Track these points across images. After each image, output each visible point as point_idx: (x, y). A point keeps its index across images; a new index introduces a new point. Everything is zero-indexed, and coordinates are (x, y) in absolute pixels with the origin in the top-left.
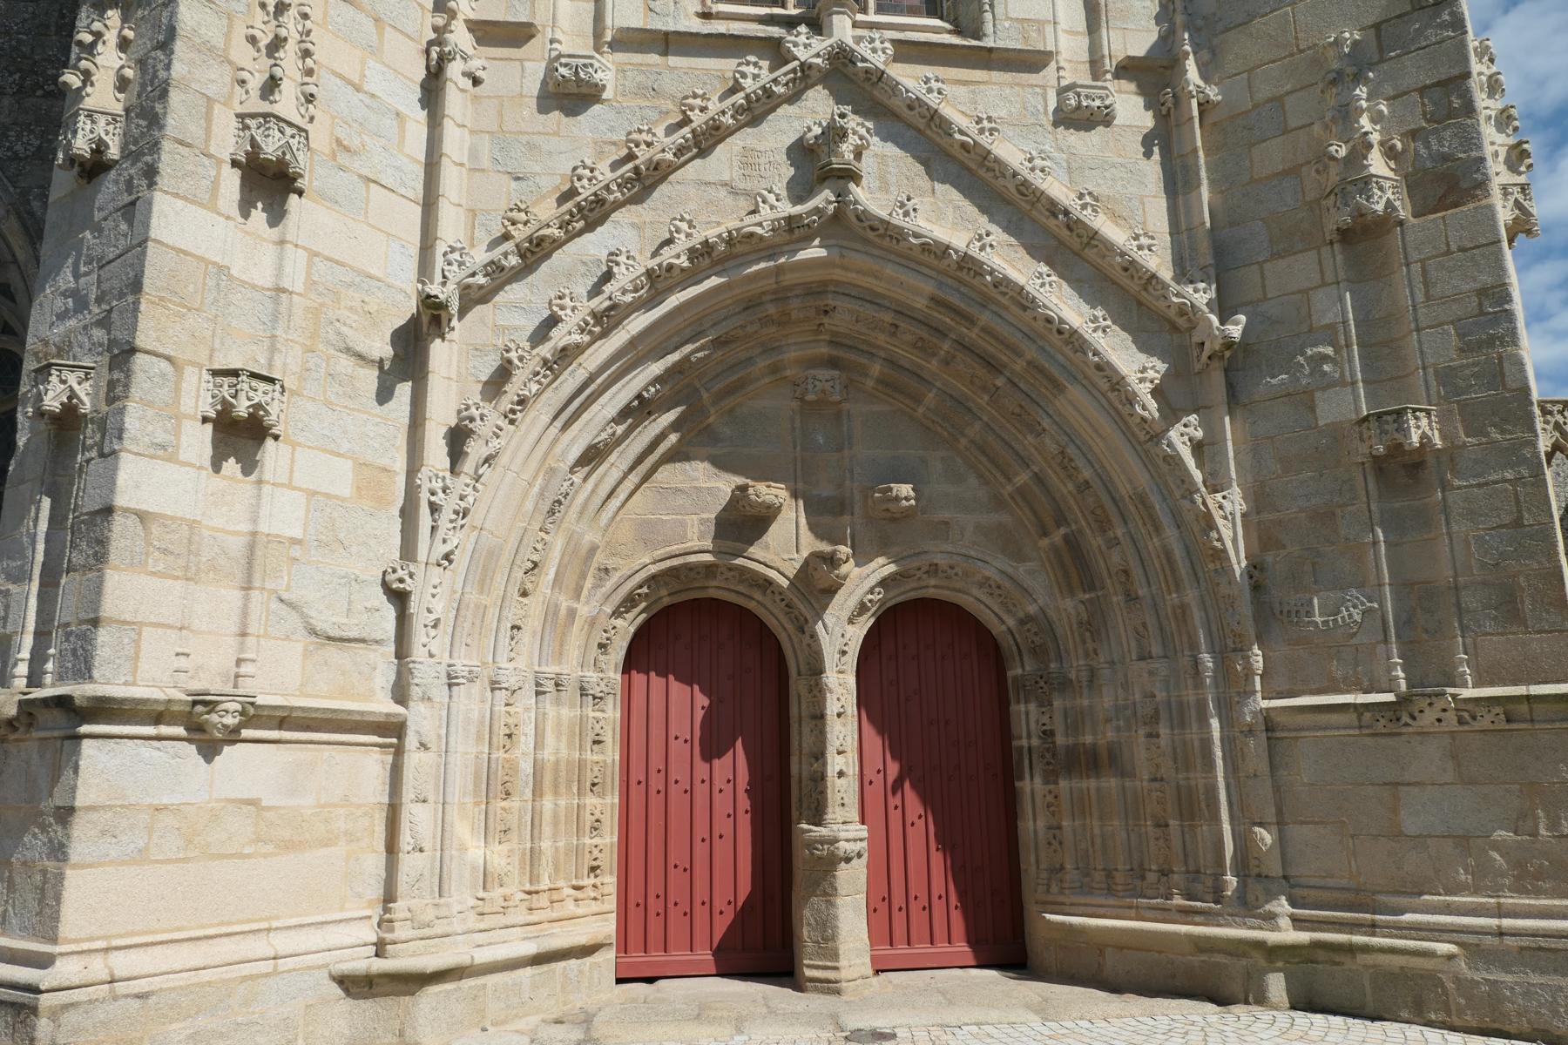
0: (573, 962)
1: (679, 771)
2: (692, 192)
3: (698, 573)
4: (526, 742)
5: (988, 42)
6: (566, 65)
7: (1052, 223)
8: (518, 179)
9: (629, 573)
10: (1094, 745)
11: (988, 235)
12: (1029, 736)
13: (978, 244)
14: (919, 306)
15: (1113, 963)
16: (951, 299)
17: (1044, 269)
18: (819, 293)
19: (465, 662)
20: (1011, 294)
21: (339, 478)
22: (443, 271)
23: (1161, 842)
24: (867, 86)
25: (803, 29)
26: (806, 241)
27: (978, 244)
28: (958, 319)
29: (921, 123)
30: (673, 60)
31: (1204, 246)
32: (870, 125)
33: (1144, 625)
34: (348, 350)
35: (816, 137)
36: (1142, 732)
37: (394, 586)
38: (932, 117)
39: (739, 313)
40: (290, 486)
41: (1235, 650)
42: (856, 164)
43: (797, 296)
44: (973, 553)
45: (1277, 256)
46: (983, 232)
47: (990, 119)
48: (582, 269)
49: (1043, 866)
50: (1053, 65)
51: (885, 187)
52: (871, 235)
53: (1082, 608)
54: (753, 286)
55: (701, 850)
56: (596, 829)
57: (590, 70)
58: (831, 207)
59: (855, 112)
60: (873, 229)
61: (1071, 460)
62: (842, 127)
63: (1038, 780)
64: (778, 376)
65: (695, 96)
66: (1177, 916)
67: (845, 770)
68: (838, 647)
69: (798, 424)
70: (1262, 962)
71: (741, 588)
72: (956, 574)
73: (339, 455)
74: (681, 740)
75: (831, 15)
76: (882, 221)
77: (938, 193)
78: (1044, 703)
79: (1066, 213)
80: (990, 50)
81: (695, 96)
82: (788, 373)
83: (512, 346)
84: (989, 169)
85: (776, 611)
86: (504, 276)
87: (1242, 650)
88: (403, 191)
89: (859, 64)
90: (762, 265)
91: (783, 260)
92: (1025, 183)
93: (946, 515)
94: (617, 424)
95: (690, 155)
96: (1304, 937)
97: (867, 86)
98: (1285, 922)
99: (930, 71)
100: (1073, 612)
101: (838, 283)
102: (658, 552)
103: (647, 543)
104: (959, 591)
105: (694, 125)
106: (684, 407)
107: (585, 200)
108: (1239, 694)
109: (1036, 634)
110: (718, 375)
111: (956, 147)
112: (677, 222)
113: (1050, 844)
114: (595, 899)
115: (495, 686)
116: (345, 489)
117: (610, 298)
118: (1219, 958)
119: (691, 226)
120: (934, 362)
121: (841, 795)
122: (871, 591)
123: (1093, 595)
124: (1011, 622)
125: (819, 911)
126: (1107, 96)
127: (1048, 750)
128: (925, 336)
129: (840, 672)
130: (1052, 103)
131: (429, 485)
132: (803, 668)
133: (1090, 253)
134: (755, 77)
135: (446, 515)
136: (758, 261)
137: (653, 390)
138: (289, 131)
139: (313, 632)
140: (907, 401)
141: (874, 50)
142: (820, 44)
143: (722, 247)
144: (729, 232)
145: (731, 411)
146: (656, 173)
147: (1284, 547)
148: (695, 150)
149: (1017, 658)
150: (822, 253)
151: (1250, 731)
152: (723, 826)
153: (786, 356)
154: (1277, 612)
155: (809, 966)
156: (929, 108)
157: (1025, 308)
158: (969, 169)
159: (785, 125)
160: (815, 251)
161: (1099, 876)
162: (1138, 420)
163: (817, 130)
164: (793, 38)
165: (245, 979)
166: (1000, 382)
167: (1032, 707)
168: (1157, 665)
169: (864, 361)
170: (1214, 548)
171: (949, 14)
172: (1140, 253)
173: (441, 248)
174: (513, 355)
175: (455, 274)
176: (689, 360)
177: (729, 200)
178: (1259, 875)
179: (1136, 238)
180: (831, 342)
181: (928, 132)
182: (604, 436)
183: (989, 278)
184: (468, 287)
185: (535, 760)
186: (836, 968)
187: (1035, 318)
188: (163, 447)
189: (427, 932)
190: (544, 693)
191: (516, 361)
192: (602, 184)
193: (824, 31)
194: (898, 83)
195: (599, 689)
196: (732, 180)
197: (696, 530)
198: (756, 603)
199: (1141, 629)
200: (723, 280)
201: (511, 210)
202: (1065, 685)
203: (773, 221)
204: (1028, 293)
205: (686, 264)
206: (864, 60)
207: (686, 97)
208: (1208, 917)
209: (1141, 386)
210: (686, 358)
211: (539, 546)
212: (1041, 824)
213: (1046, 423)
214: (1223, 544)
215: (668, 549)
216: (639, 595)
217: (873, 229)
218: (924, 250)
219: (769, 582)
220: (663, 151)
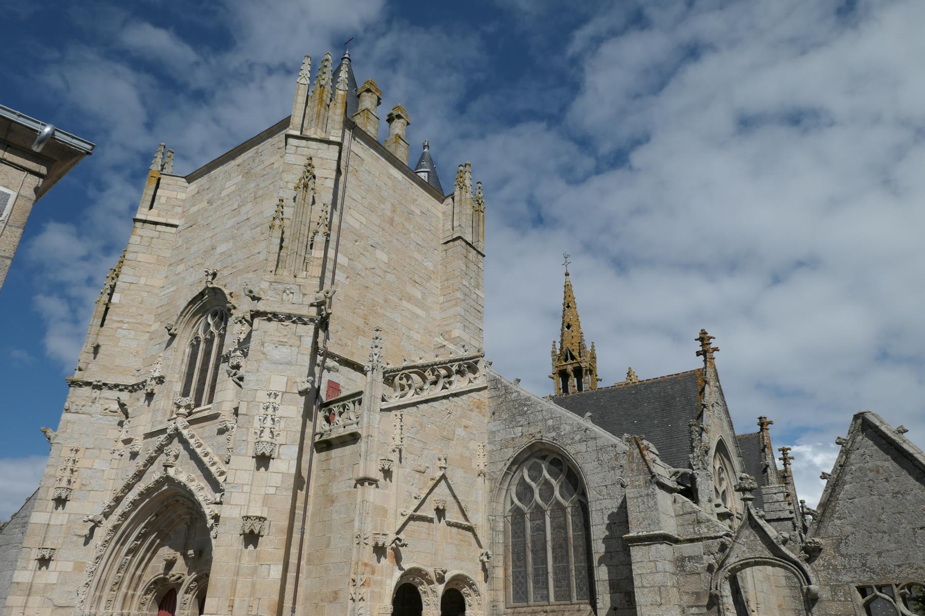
21: (69, 566)
34: (76, 535)
40: (55, 571)
116: (70, 570)
122: (191, 583)
138: (62, 489)
188: (25, 567)
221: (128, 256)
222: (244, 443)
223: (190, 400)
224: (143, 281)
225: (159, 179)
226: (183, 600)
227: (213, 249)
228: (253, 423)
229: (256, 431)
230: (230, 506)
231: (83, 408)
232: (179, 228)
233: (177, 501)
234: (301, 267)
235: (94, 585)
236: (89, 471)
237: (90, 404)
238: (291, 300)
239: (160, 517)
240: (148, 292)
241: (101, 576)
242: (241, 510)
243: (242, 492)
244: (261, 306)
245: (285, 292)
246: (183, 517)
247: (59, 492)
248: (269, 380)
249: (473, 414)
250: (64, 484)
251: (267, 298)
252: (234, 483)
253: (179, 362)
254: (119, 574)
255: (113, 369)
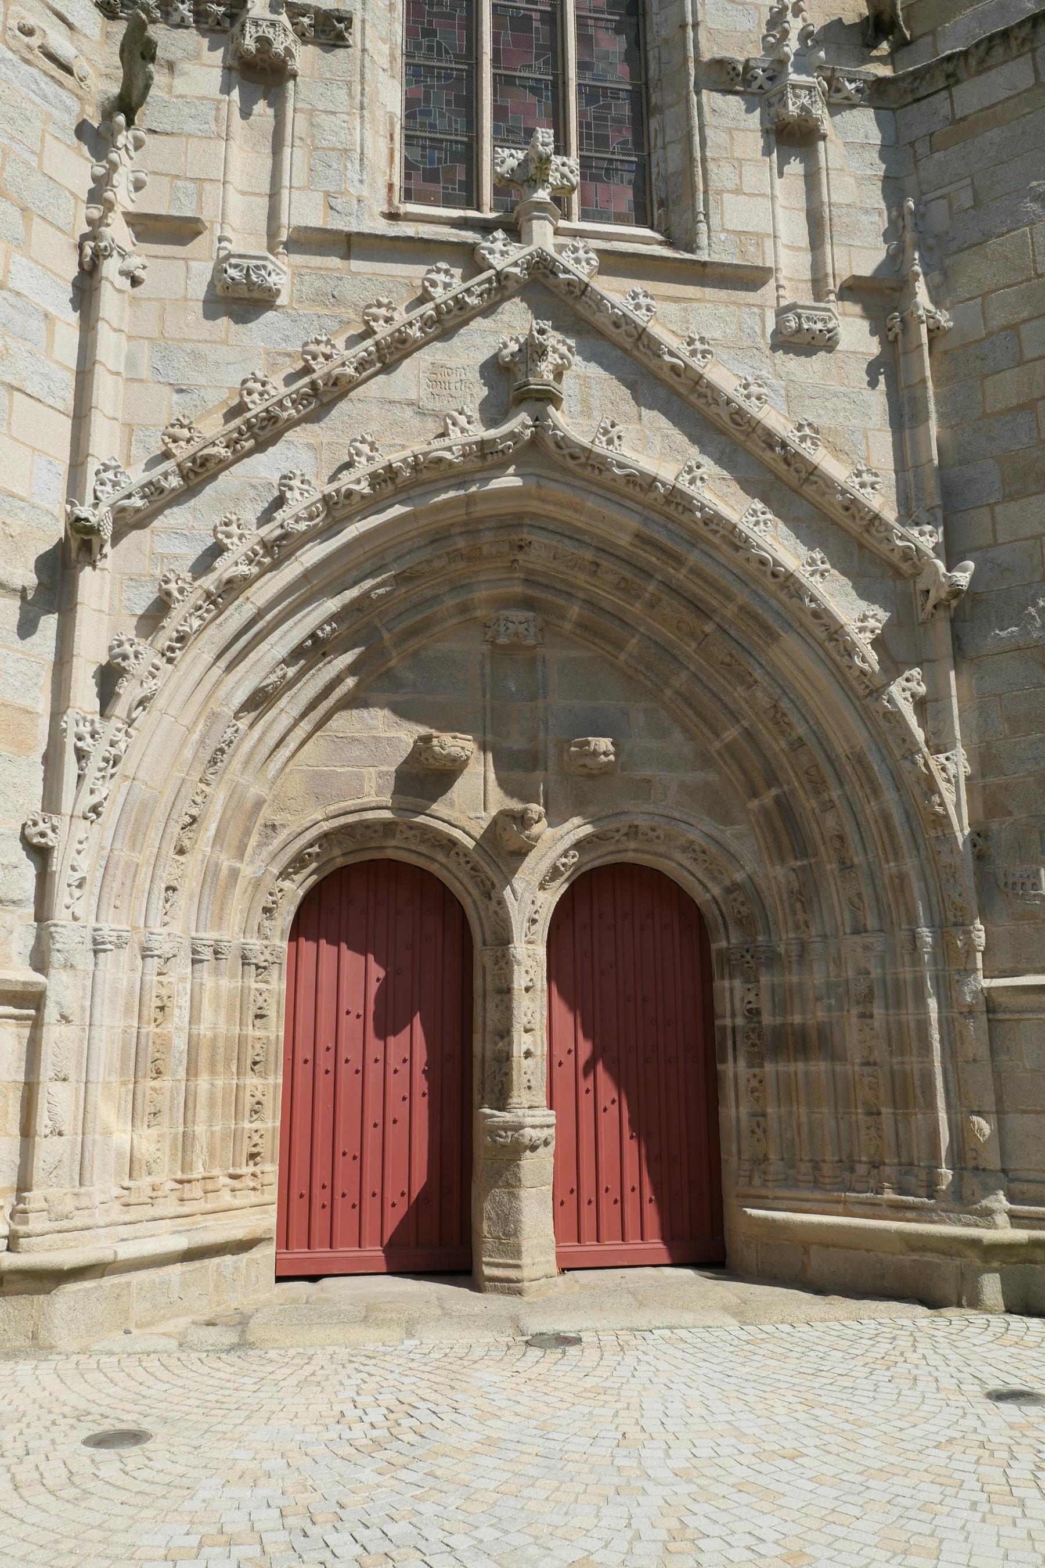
0: (228, 1259)
1: (350, 1050)
2: (375, 411)
3: (375, 831)
4: (180, 1015)
5: (702, 256)
6: (236, 266)
7: (768, 455)
8: (180, 391)
9: (299, 830)
10: (803, 1027)
11: (698, 467)
12: (733, 1015)
13: (688, 477)
14: (622, 543)
15: (817, 1262)
16: (657, 536)
17: (759, 505)
18: (512, 526)
19: (113, 927)
20: (722, 532)
22: (95, 491)
23: (873, 1130)
24: (569, 300)
25: (499, 234)
26: (500, 468)
27: (688, 477)
28: (664, 558)
29: (628, 343)
30: (356, 265)
31: (931, 484)
32: (571, 342)
33: (859, 895)
35: (513, 355)
36: (854, 1012)
37: (35, 841)
38: (640, 336)
39: (425, 546)
41: (955, 924)
42: (556, 385)
43: (489, 529)
44: (676, 815)
45: (1008, 498)
46: (693, 464)
47: (702, 340)
48: (252, 493)
49: (745, 1156)
50: (772, 283)
51: (587, 411)
52: (571, 463)
53: (792, 876)
54: (441, 517)
55: (372, 1136)
56: (256, 1112)
57: (263, 272)
58: (528, 432)
59: (556, 328)
60: (573, 457)
61: (784, 715)
62: (541, 344)
63: (742, 1063)
64: (468, 617)
65: (379, 305)
66: (888, 1212)
67: (532, 1049)
68: (527, 915)
69: (488, 670)
70: (978, 1262)
71: (422, 849)
72: (658, 837)
74: (353, 1015)
75: (531, 220)
76: (584, 449)
77: (645, 419)
78: (751, 979)
79: (784, 445)
80: (704, 264)
81: (379, 305)
82: (478, 613)
83: (172, 576)
84: (701, 395)
85: (460, 875)
86: (165, 498)
87: (963, 925)
88: (50, 401)
89: (561, 276)
90: (451, 494)
91: (474, 489)
92: (740, 411)
93: (647, 773)
94: (288, 666)
95: (373, 370)
96: (1022, 1235)
97: (569, 300)
98: (1002, 1219)
99: (638, 285)
100: (783, 881)
101: (534, 516)
102: (332, 808)
103: (319, 798)
104: (661, 855)
105: (377, 337)
106: (362, 649)
107: (256, 416)
108: (959, 971)
109: (743, 904)
110: (401, 614)
111: (666, 369)
112: (358, 444)
113: (753, 1132)
114: (254, 1189)
115: (146, 953)
117: (282, 526)
118: (930, 1258)
119: (373, 448)
120: (638, 605)
121: (527, 1077)
122: (565, 855)
123: (805, 862)
124: (716, 891)
125: (500, 1204)
126: (830, 319)
127: (753, 1030)
128: (629, 576)
129: (530, 942)
130: (771, 326)
131: (75, 729)
132: (489, 938)
133: (808, 490)
134: (447, 286)
135: (95, 762)
136: (446, 489)
137: (328, 628)
140: (609, 648)
141: (577, 261)
142: (518, 252)
143: (407, 473)
144: (415, 456)
145: (415, 654)
146: (335, 389)
147: (1010, 814)
148: (379, 365)
149: (722, 930)
150: (517, 482)
151: (970, 1013)
152: (398, 1109)
153: (476, 595)
154: (1002, 885)
155: (488, 1264)
156: (636, 326)
157: (737, 548)
158: (678, 394)
159: (478, 340)
160: (509, 480)
161: (805, 1167)
162: (857, 673)
163: (514, 347)
164: (488, 244)
166: (709, 628)
167: (737, 983)
168: (872, 940)
169: (560, 601)
170: (936, 814)
171: (660, 223)
172: (862, 491)
173: (93, 466)
174: (172, 587)
175: (109, 496)
176: (369, 597)
177: (416, 422)
178: (976, 1168)
179: (859, 474)
180: (526, 580)
181: (635, 353)
182: (273, 678)
183: (698, 514)
184: (123, 509)
185: (190, 1035)
186: (517, 1267)
187: (748, 560)
189: (65, 1224)
190: (202, 961)
191: (176, 594)
192: (275, 400)
193: (523, 237)
194: (603, 298)
195: (263, 958)
196: (420, 399)
197: (373, 784)
198: (438, 866)
199: (856, 900)
200: (407, 509)
201: (173, 426)
202: (772, 960)
203: (463, 445)
204: (741, 532)
205: (367, 490)
206: (566, 271)
207: (369, 306)
208: (921, 1213)
209: (861, 636)
210: (366, 595)
211: (199, 799)
212: (744, 1111)
213: (758, 674)
214: (945, 809)
215: (342, 804)
216: (310, 855)
217: (573, 457)
218: (628, 482)
219: (453, 842)
220: (343, 364)
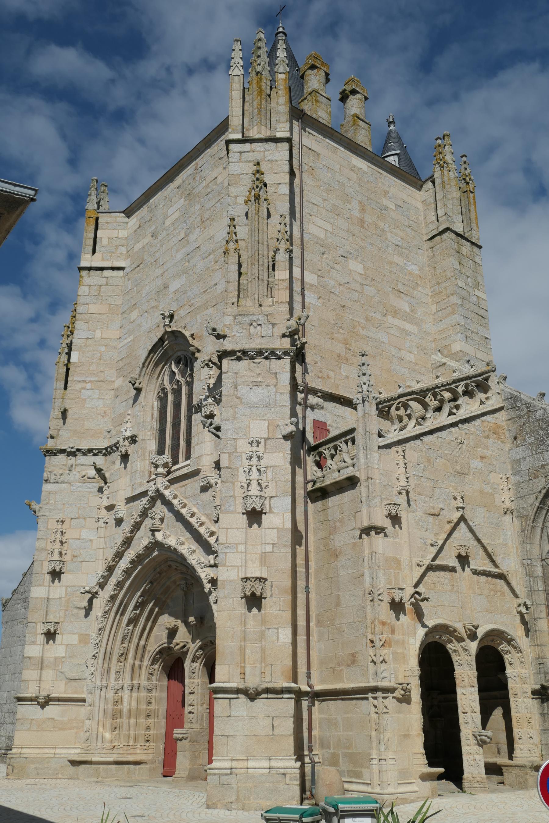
0: (132, 766)
21: (74, 639)
26: (153, 551)
34: (76, 607)
40: (62, 644)
73: (74, 634)
88: (92, 560)
116: (76, 642)
122: (197, 651)
139: (67, 679)
143: (136, 559)
165: (47, 758)
182: (132, 615)
188: (33, 642)
189: (87, 752)
205: (131, 566)
221: (80, 309)
222: (232, 499)
223: (167, 457)
224: (98, 334)
225: (97, 219)
226: (192, 668)
227: (165, 288)
228: (238, 476)
229: (242, 484)
230: (226, 568)
231: (62, 477)
232: (127, 270)
233: (170, 566)
234: (265, 294)
235: (101, 656)
236: (78, 542)
237: (68, 472)
238: (259, 333)
239: (155, 584)
240: (105, 346)
241: (106, 648)
242: (238, 572)
243: (237, 552)
244: (227, 345)
245: (251, 324)
246: (178, 583)
247: (53, 565)
248: (248, 427)
249: (490, 441)
250: (56, 556)
251: (233, 334)
252: (227, 543)
253: (149, 418)
254: (123, 645)
255: (84, 433)
